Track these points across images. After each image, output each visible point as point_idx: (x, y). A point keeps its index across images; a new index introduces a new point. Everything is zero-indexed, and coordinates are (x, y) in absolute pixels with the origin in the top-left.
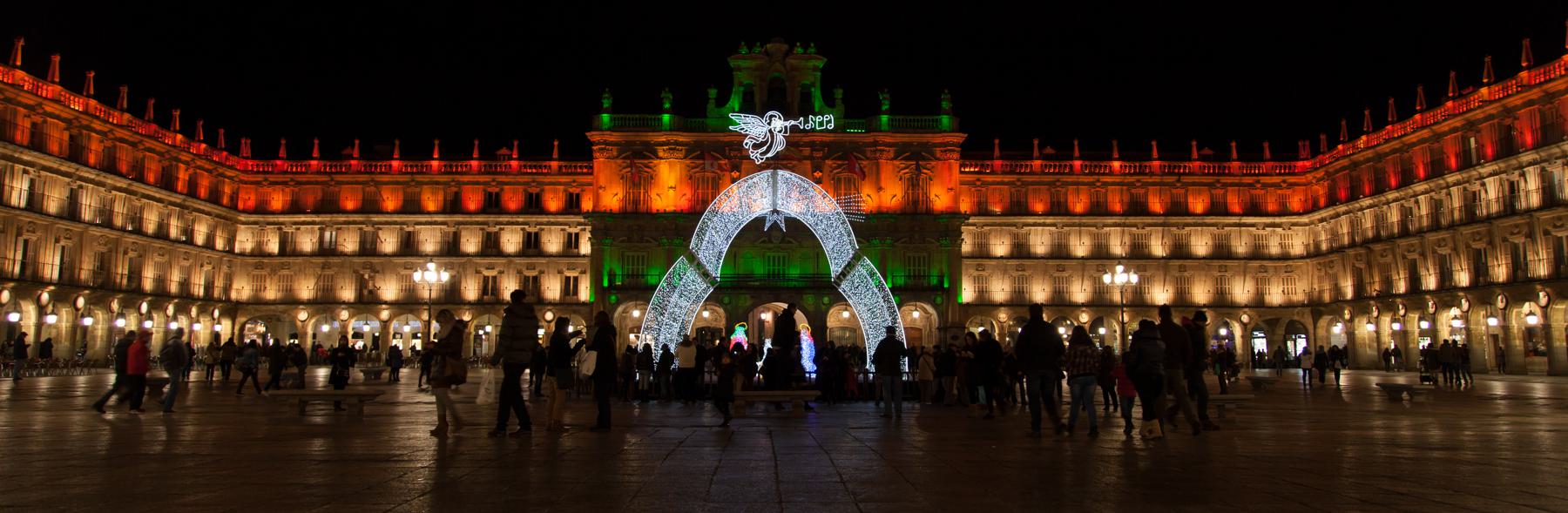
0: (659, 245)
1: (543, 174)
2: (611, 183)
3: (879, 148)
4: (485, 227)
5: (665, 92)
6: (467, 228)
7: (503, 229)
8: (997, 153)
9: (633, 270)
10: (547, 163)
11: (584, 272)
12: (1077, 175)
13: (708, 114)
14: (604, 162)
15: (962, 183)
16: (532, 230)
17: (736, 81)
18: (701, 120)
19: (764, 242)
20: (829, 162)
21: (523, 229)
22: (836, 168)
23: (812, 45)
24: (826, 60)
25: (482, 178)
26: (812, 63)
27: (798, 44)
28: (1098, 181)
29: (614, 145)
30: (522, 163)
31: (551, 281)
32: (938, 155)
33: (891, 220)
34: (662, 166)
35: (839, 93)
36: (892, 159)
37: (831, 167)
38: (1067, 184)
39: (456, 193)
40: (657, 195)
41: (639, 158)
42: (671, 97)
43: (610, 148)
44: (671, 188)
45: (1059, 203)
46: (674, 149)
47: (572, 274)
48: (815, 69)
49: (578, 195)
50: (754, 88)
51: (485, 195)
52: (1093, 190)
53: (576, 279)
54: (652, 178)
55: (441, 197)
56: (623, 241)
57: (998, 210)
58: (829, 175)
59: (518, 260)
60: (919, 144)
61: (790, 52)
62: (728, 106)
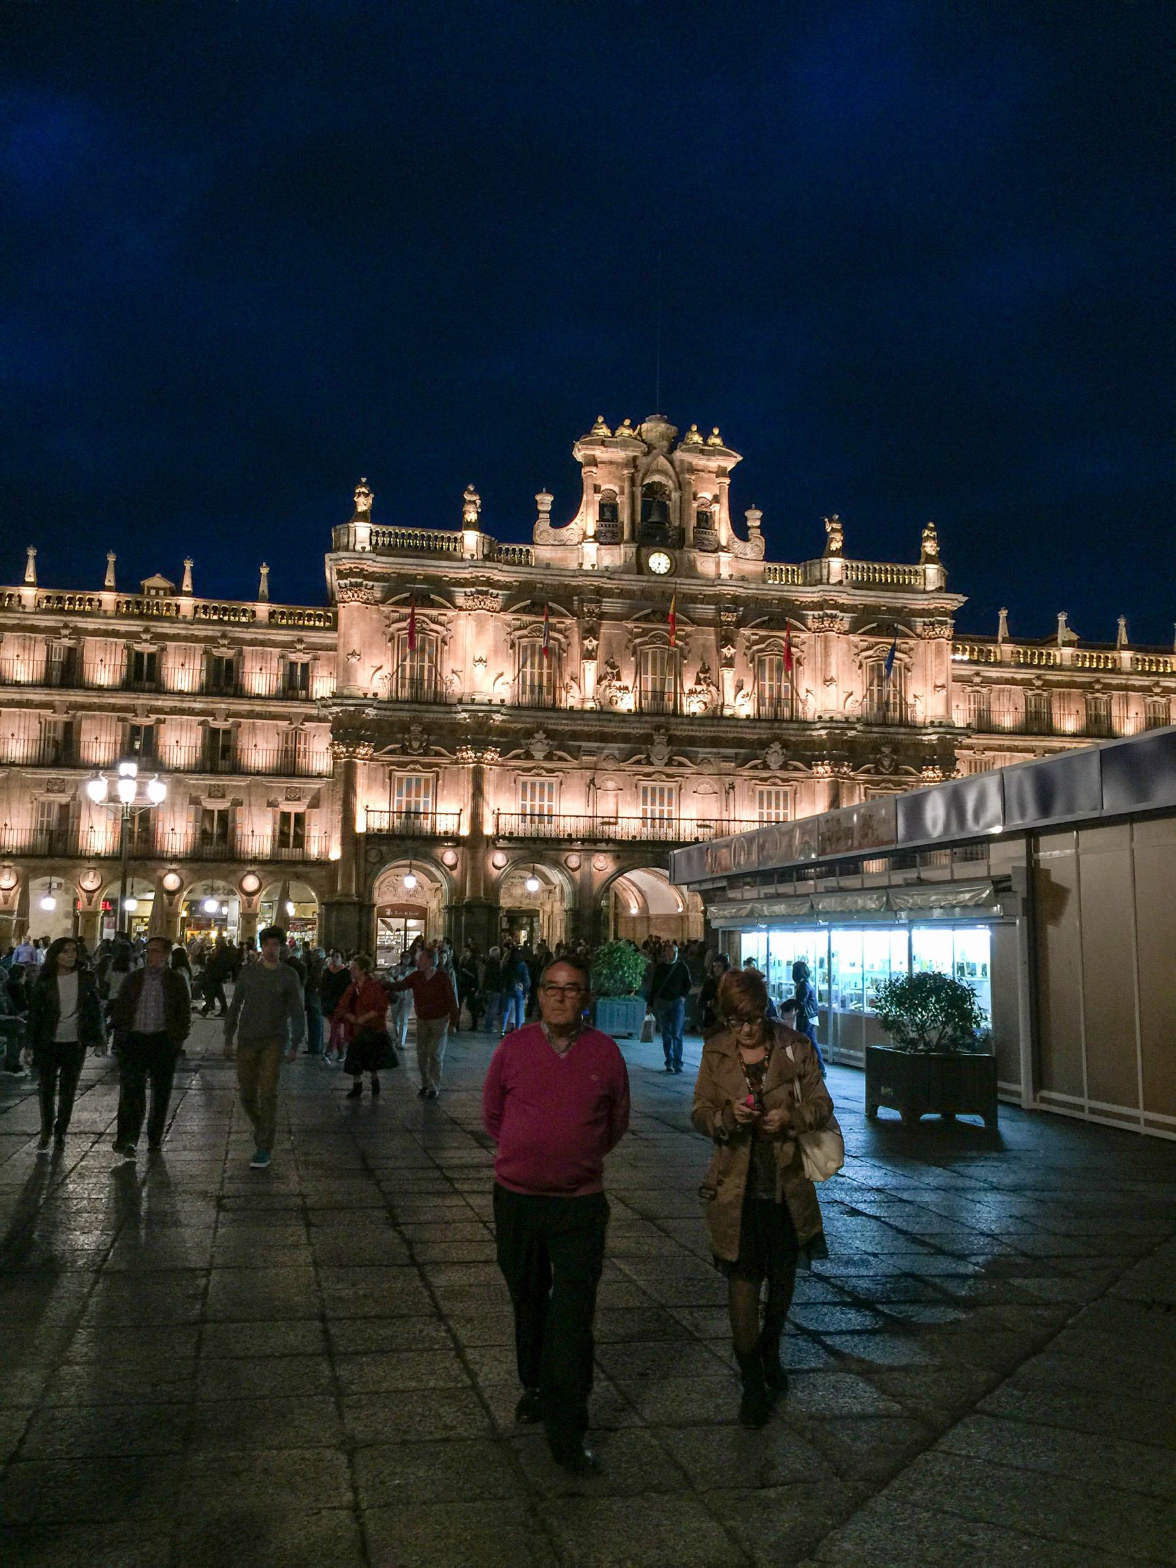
0: (457, 763)
1: (239, 624)
2: (370, 646)
3: (829, 612)
4: (129, 715)
5: (471, 493)
6: (94, 717)
7: (164, 722)
8: (1003, 631)
9: (408, 803)
10: (248, 606)
11: (315, 804)
12: (1127, 674)
13: (537, 539)
14: (359, 607)
15: (956, 679)
16: (220, 724)
17: (588, 484)
18: (524, 548)
19: (638, 762)
20: (742, 631)
21: (201, 723)
22: (756, 643)
23: (716, 431)
24: (740, 458)
25: (123, 626)
26: (714, 463)
27: (694, 428)
28: (1157, 684)
29: (376, 580)
30: (201, 602)
31: (255, 820)
32: (919, 630)
33: (852, 733)
34: (462, 622)
35: (754, 517)
36: (846, 633)
37: (748, 640)
38: (1108, 687)
39: (71, 651)
40: (453, 672)
41: (423, 606)
42: (478, 502)
43: (371, 583)
44: (481, 660)
45: (1097, 716)
46: (486, 593)
47: (293, 808)
48: (721, 472)
49: (305, 667)
50: (618, 500)
51: (129, 656)
52: (1149, 700)
53: (300, 818)
54: (444, 642)
55: (40, 654)
56: (391, 752)
57: (1008, 722)
58: (745, 654)
59: (192, 780)
60: (891, 610)
61: (675, 443)
62: (572, 525)
